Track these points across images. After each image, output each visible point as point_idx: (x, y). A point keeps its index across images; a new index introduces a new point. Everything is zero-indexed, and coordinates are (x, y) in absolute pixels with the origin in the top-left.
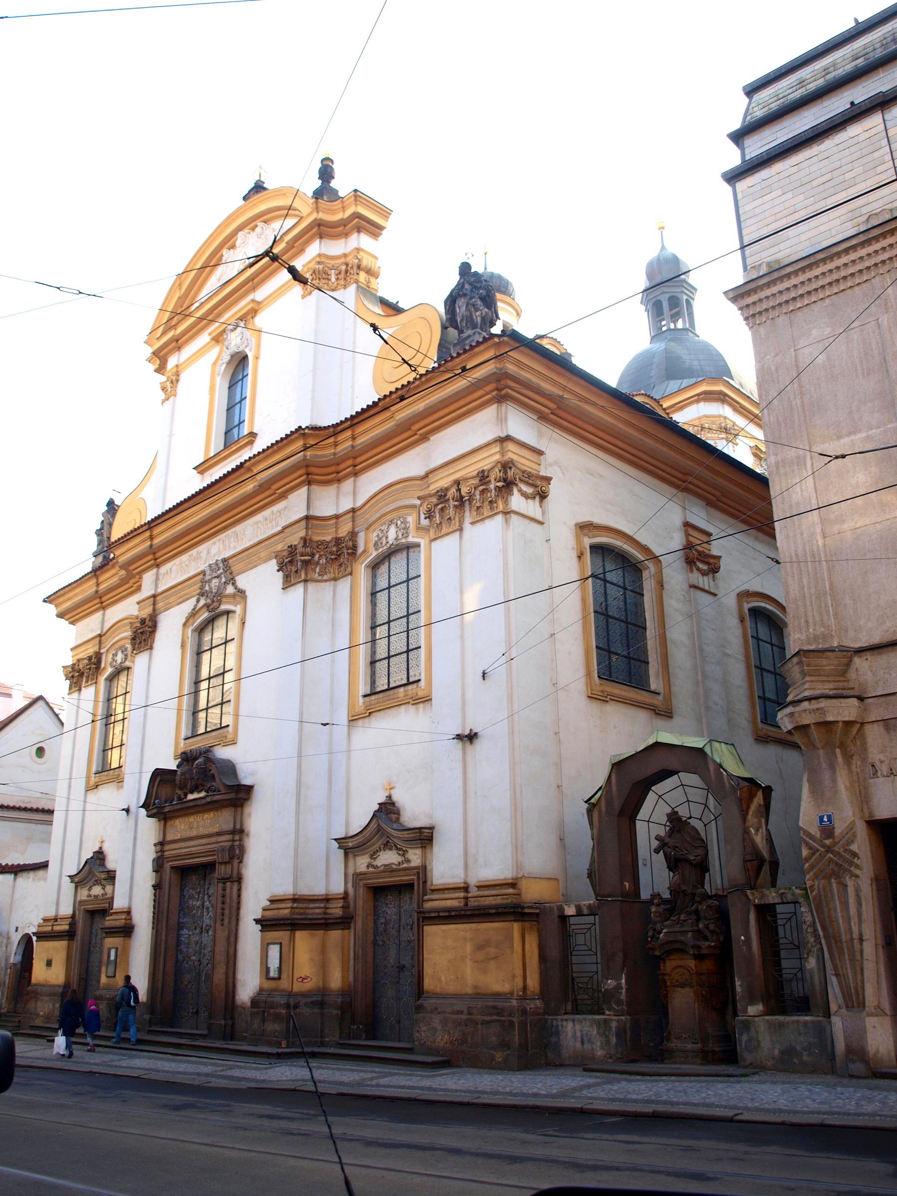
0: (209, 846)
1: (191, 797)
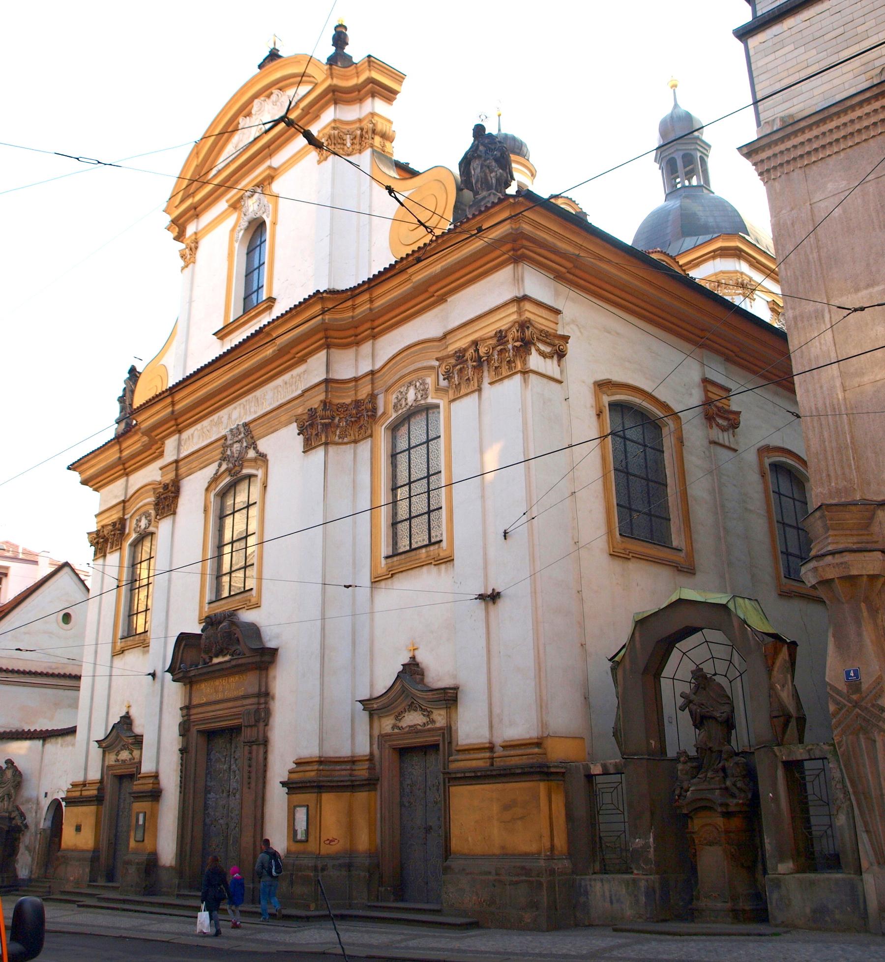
0: (235, 710)
1: (216, 660)
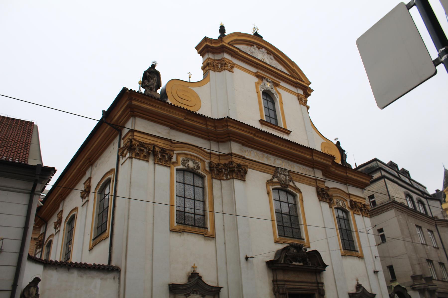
0: (311, 287)
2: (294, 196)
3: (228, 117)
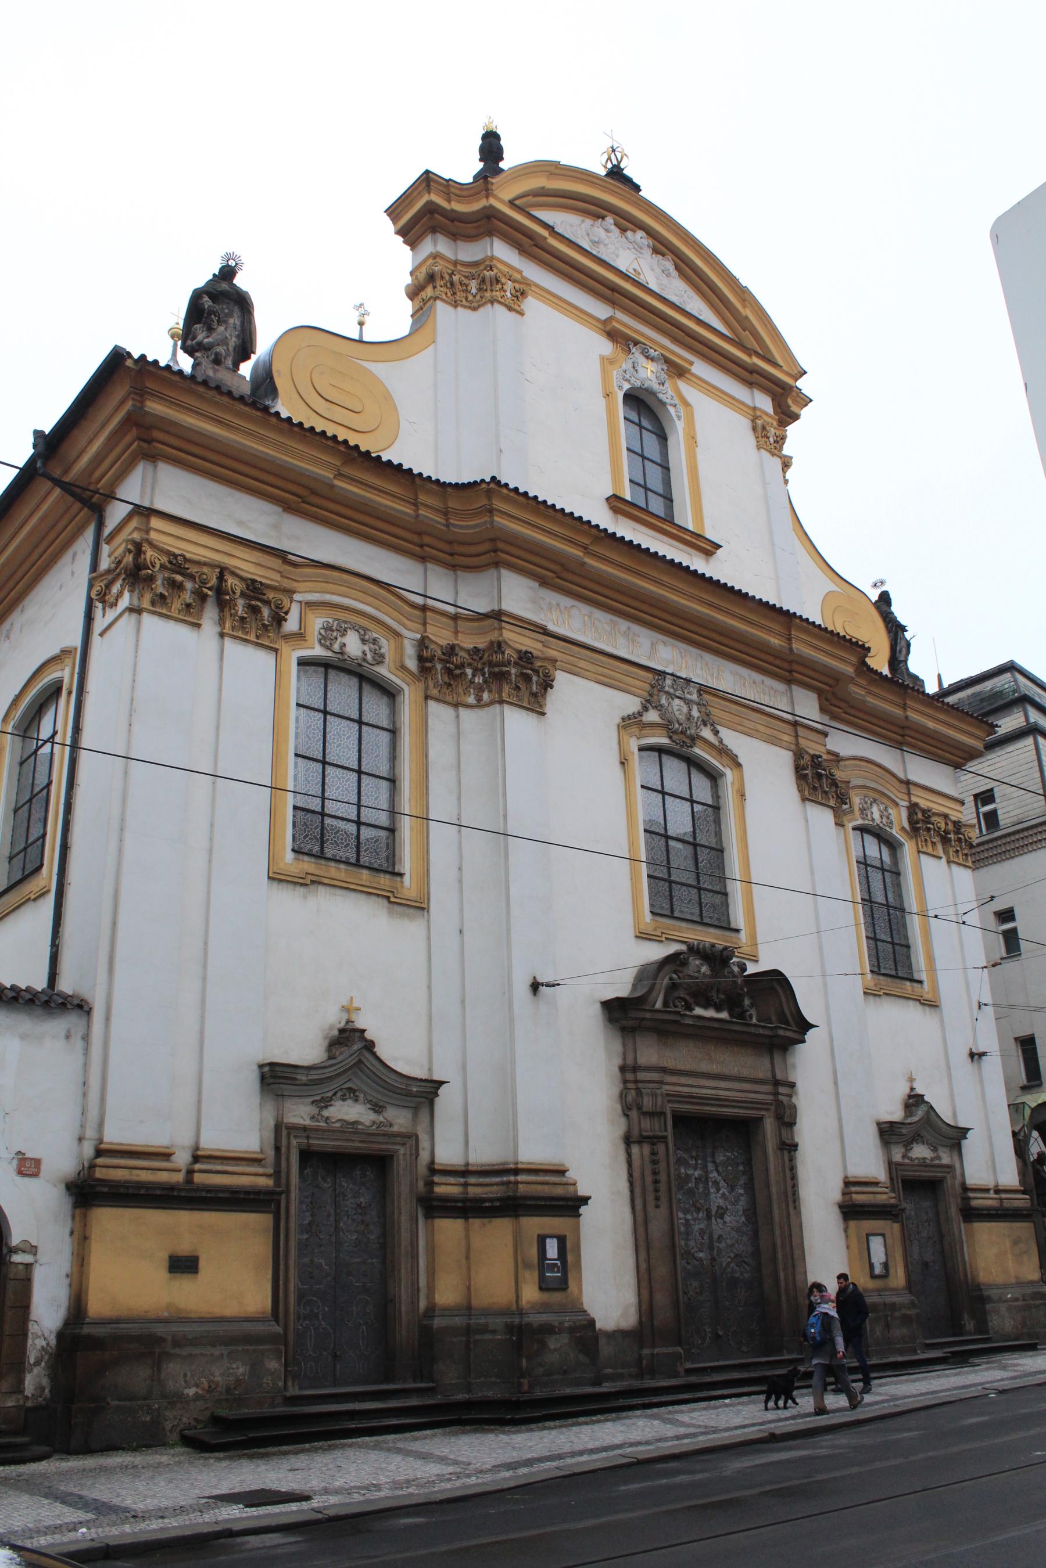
0: (752, 1095)
2: (713, 777)
3: (493, 478)
